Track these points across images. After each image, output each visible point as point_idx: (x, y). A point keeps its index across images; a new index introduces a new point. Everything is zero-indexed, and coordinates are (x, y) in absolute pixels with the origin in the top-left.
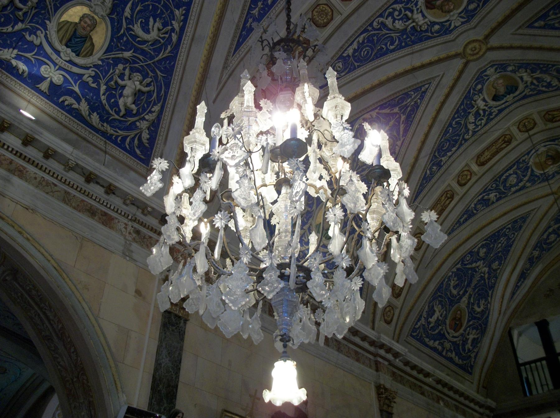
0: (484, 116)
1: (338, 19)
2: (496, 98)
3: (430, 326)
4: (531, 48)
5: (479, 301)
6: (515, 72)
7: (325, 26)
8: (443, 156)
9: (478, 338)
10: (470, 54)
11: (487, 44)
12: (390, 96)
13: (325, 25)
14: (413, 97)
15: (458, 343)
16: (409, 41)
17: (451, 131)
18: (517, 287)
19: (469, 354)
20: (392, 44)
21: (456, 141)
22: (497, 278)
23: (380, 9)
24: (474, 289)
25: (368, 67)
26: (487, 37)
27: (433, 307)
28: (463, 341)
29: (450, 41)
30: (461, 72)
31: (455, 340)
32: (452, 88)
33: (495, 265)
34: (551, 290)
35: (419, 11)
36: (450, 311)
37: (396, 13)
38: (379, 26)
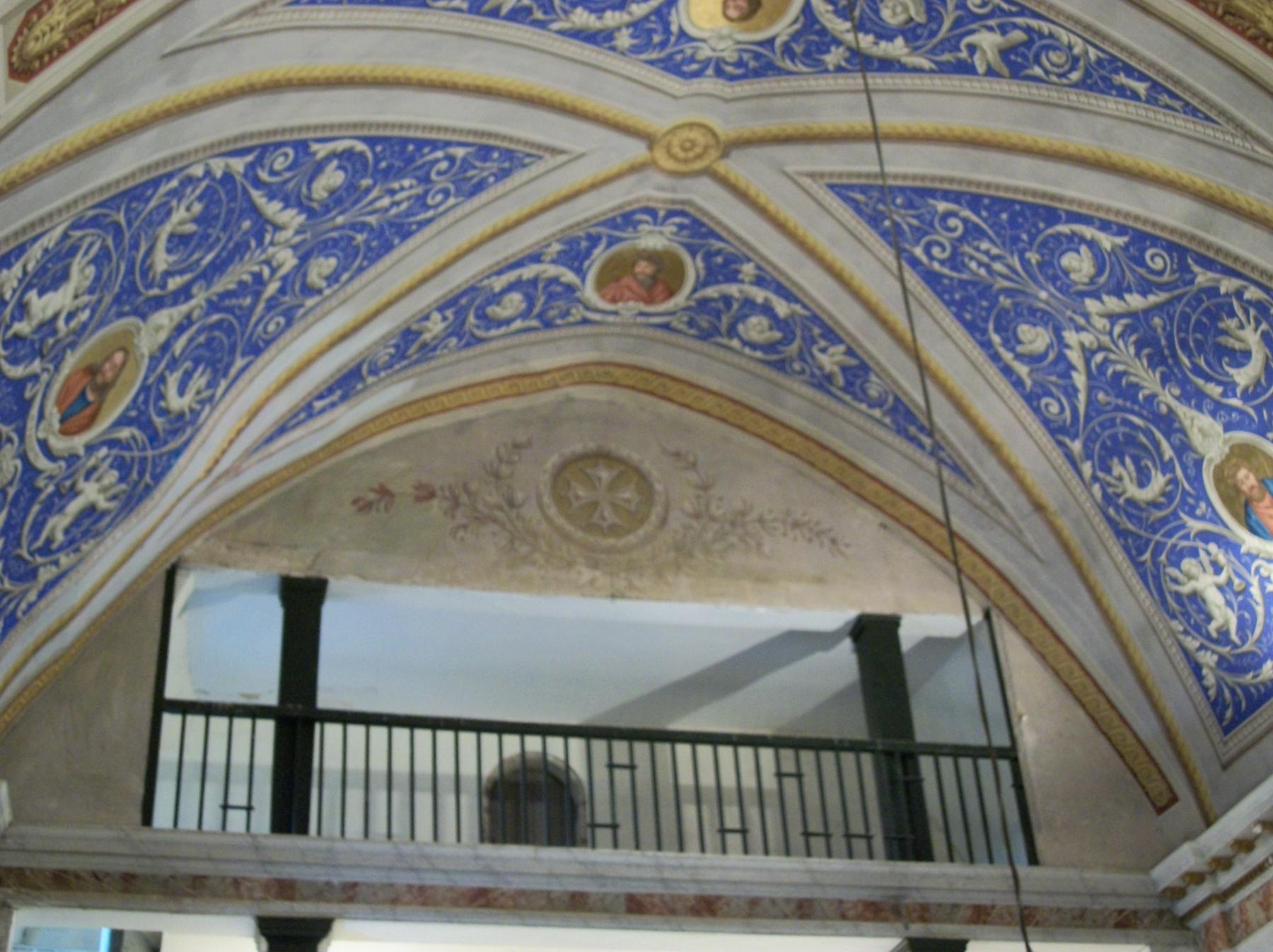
5: (195, 369)
9: (104, 513)
15: (41, 483)
18: (306, 411)
19: (39, 559)
22: (289, 323)
24: (213, 306)
27: (73, 251)
28: (58, 493)
31: (41, 462)
33: (322, 267)
34: (384, 492)
36: (102, 324)
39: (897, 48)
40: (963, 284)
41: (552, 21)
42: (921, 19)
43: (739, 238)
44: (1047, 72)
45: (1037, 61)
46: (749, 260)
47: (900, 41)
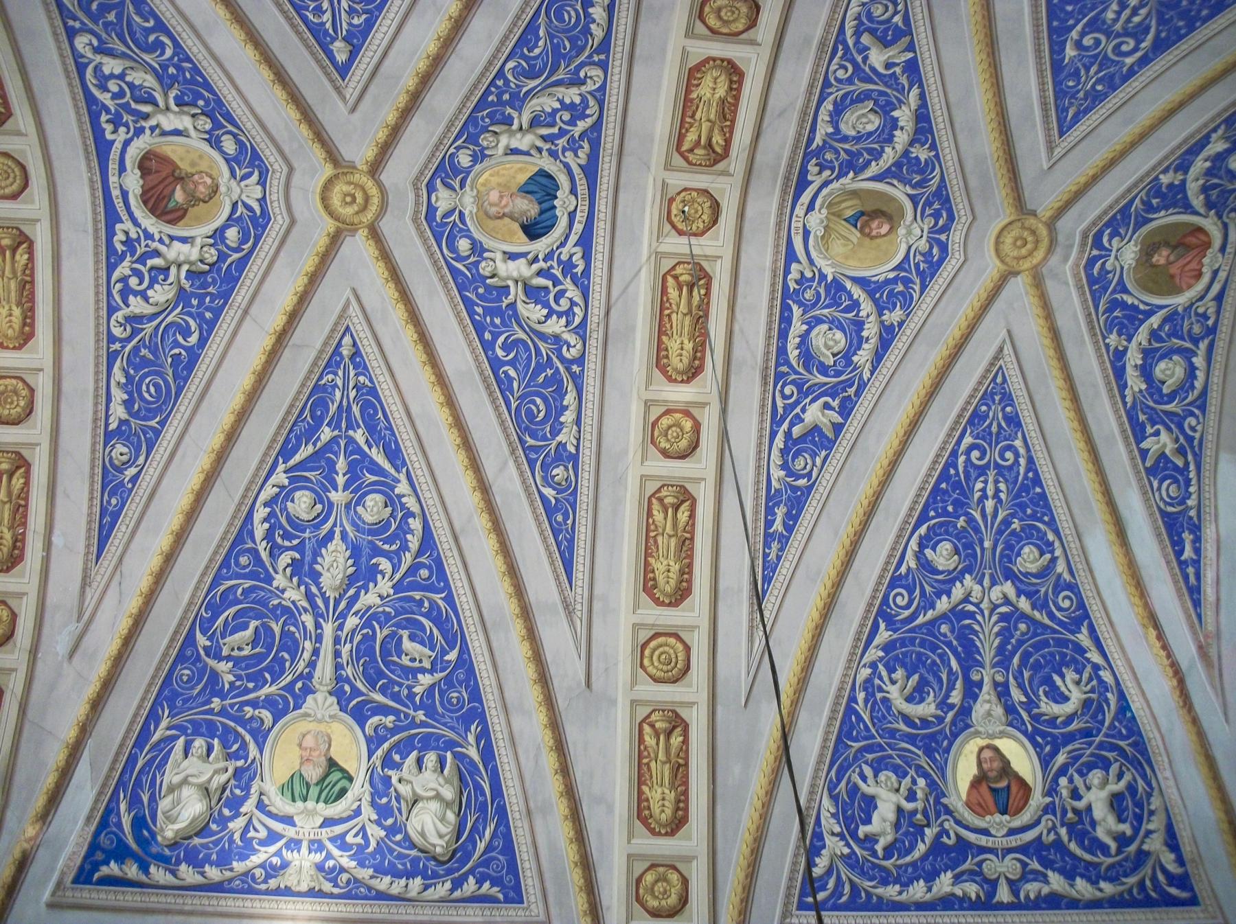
0: (556, 282)
1: (43, 386)
2: (533, 231)
3: (879, 848)
4: (416, 98)
6: (484, 156)
7: (31, 412)
8: (555, 432)
9: (1131, 788)
10: (357, 213)
11: (354, 167)
12: (284, 420)
13: (29, 411)
14: (340, 383)
16: (212, 301)
17: (512, 373)
20: (186, 333)
21: (555, 380)
23: (97, 301)
25: (182, 409)
26: (333, 156)
29: (288, 231)
30: (385, 256)
31: (1030, 836)
32: (405, 296)
35: (167, 241)
37: (133, 282)
38: (129, 328)
39: (904, 115)
40: (1161, 21)
41: (861, 378)
42: (871, 104)
43: (1129, 190)
44: (896, 13)
45: (889, 20)
46: (1157, 178)
47: (896, 114)
